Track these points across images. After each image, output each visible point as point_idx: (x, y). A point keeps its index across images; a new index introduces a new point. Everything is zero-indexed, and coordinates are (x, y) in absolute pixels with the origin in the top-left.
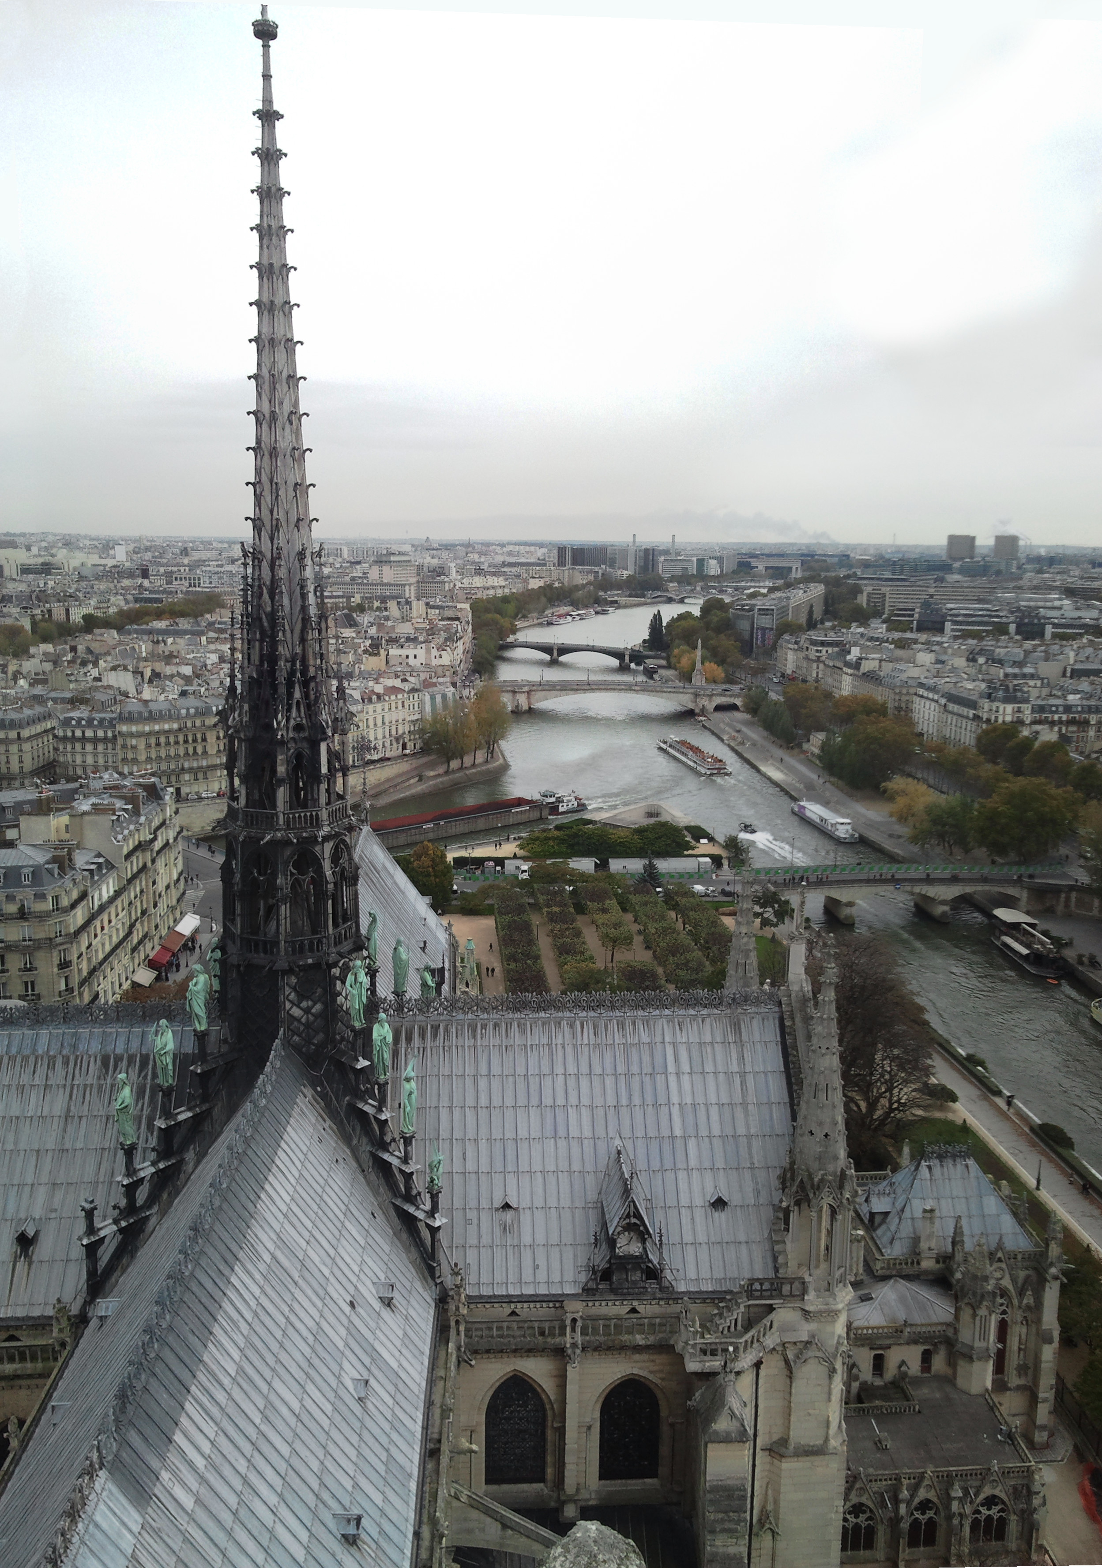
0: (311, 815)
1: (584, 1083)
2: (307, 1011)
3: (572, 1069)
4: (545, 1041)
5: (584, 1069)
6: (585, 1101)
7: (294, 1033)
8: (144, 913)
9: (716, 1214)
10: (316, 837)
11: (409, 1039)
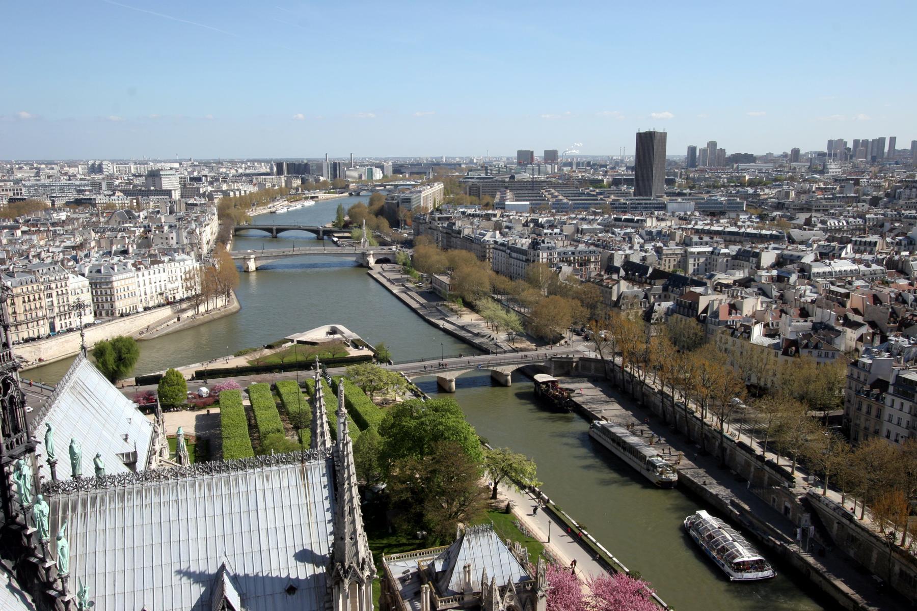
1: (201, 522)
3: (192, 515)
4: (173, 498)
5: (201, 513)
6: (201, 534)
9: (289, 597)
11: (74, 509)
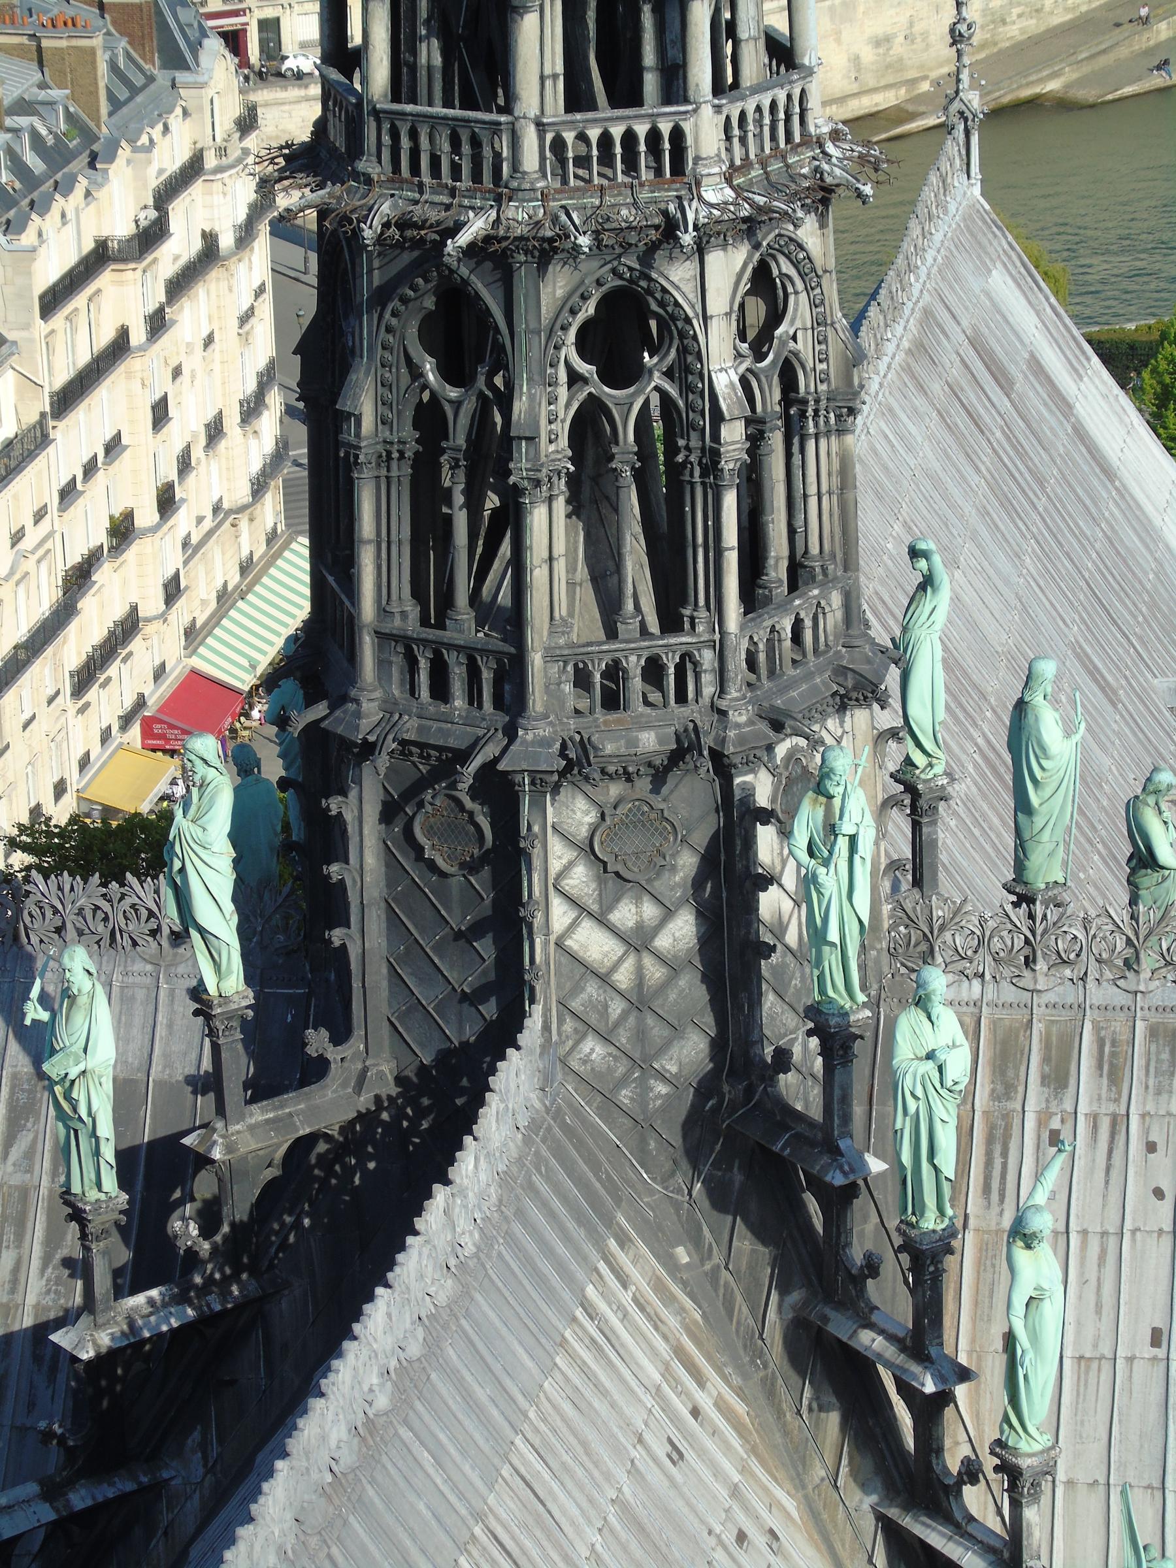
0: (654, 136)
2: (638, 941)
7: (586, 1027)
8: (123, 531)
10: (670, 228)
11: (1058, 1078)
